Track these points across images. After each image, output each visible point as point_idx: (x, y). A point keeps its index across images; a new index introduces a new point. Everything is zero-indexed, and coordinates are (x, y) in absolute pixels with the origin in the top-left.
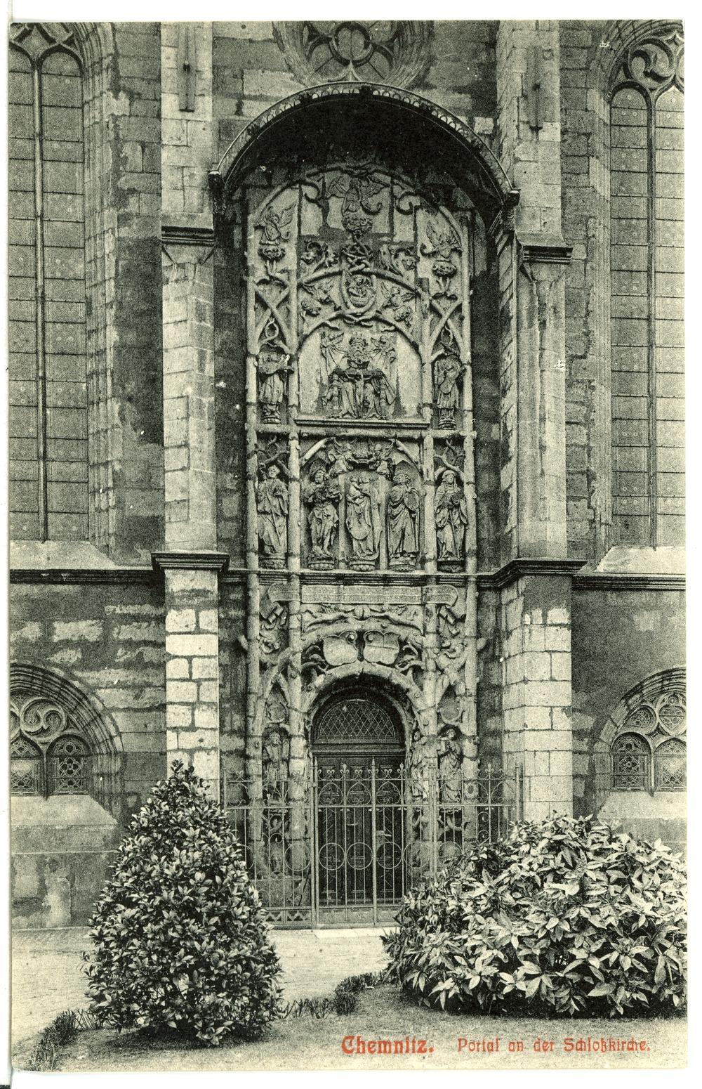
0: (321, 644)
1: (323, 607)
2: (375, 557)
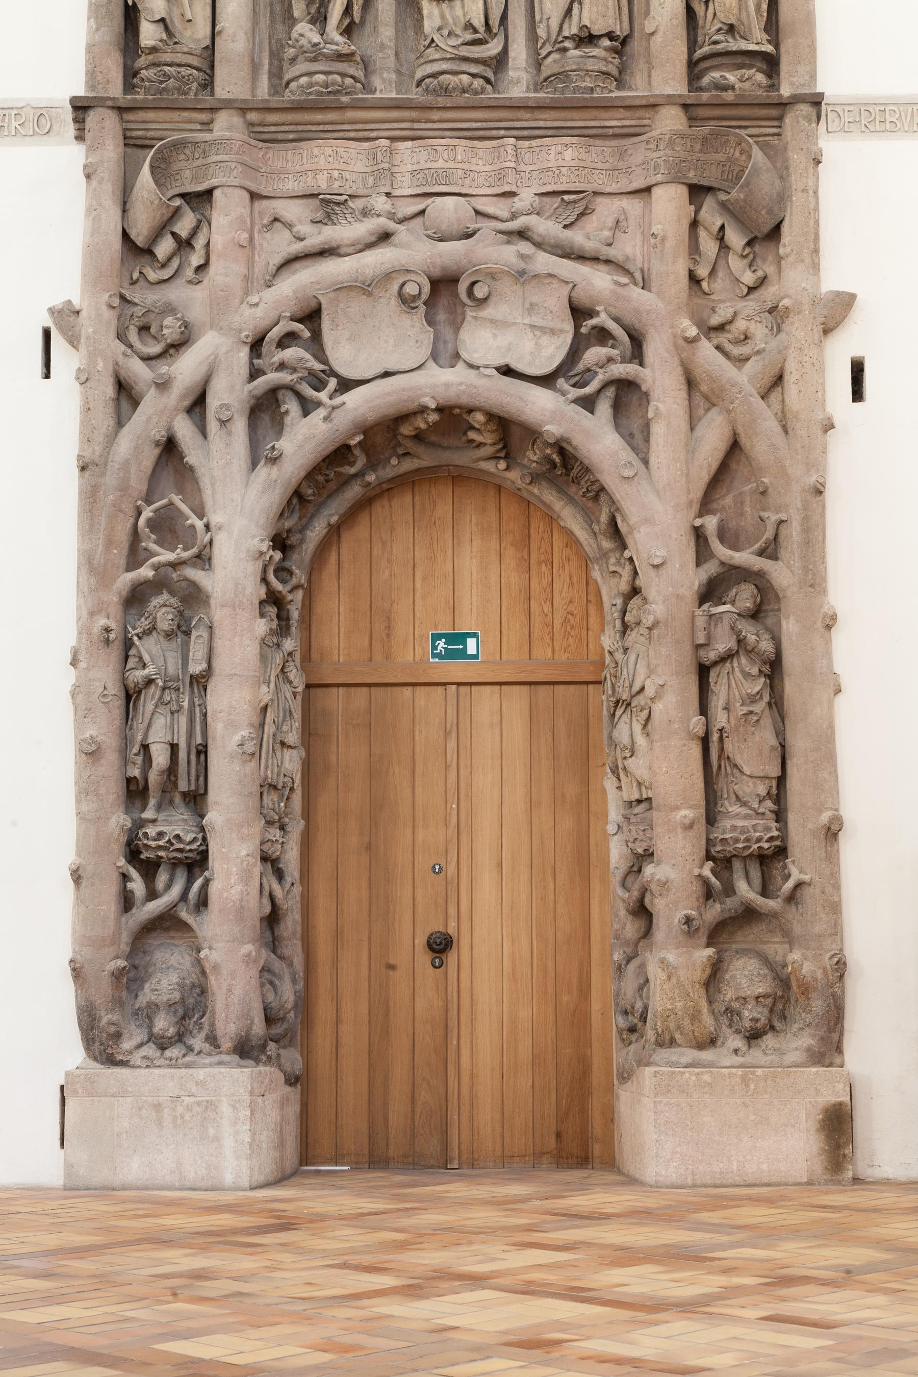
0: (312, 316)
1: (330, 206)
2: (493, 48)
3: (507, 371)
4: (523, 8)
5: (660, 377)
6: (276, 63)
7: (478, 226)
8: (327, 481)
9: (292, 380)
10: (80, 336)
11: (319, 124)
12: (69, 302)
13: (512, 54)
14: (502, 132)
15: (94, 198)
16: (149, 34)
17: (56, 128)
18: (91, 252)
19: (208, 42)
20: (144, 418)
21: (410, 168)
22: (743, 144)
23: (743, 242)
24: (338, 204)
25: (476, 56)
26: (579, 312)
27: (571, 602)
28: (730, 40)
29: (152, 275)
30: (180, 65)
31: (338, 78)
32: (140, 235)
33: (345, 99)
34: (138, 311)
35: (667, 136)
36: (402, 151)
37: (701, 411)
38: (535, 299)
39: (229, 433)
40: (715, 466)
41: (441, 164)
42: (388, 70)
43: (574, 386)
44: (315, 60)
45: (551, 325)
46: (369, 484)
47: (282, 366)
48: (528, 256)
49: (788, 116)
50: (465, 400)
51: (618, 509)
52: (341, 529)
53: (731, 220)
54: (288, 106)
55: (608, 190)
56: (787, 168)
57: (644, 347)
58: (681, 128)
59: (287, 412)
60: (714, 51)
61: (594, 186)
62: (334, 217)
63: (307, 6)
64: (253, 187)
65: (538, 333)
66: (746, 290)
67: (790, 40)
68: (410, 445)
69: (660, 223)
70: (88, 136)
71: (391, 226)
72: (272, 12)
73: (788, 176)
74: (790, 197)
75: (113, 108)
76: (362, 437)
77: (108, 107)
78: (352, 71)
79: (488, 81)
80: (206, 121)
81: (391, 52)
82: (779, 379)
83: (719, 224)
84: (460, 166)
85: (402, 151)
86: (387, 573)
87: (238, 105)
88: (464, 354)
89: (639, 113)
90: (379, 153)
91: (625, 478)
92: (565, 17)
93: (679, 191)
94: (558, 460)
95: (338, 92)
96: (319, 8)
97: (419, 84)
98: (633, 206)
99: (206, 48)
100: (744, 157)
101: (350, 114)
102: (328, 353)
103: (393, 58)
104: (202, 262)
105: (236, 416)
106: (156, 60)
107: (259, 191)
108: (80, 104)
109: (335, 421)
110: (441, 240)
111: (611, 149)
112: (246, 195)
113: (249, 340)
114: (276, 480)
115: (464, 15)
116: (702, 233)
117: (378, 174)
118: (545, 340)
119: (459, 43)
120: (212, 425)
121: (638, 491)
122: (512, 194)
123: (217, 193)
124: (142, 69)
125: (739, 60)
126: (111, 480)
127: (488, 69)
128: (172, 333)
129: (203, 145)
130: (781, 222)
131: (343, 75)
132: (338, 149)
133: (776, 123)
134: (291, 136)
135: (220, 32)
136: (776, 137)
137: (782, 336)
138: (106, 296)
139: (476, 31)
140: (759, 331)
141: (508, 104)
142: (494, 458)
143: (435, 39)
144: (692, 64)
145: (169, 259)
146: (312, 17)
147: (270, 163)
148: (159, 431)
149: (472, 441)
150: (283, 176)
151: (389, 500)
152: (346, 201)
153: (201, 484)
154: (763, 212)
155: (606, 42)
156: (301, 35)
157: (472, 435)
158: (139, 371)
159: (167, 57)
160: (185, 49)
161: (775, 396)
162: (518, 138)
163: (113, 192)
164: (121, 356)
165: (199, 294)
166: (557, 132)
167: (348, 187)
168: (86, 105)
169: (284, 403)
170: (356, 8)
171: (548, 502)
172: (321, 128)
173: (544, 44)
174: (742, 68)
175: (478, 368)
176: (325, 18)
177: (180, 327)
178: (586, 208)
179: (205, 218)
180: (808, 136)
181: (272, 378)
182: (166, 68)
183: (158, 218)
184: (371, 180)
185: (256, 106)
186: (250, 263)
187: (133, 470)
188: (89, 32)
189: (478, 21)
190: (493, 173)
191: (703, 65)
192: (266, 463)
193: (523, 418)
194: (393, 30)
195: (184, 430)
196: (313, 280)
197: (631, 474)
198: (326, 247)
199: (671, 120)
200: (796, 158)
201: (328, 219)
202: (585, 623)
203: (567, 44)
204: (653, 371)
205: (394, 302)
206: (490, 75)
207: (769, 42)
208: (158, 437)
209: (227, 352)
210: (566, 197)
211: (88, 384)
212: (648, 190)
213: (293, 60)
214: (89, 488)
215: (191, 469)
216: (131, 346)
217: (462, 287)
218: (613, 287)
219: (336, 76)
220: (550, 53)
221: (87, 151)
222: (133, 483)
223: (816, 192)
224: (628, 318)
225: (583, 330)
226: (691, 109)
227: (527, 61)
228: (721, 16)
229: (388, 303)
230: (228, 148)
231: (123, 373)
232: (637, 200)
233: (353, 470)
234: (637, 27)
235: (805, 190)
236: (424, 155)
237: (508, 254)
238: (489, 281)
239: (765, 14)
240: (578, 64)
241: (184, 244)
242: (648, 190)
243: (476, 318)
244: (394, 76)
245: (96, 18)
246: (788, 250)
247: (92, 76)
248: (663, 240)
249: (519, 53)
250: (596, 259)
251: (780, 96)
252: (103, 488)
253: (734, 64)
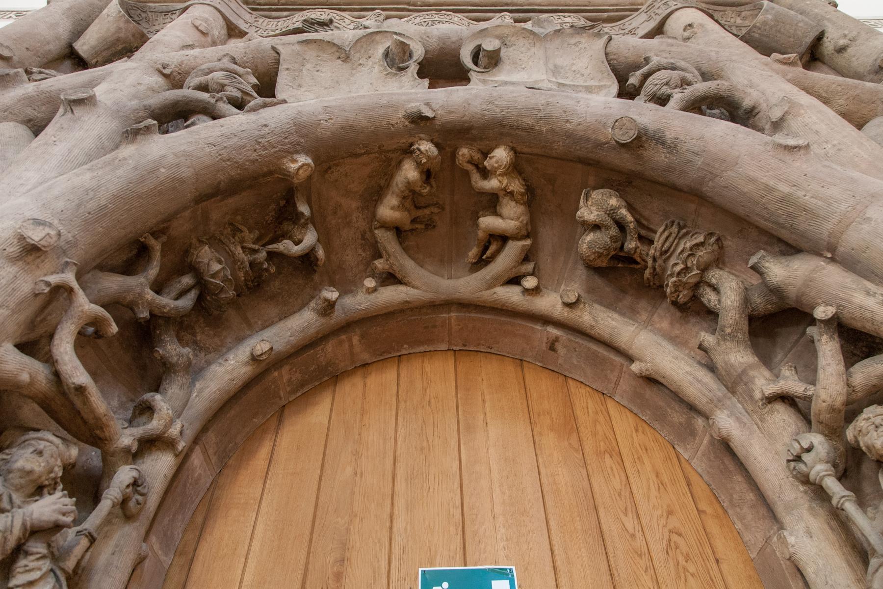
27: (670, 513)
38: (560, 61)
52: (286, 412)
86: (349, 471)
151: (365, 377)
202: (708, 550)
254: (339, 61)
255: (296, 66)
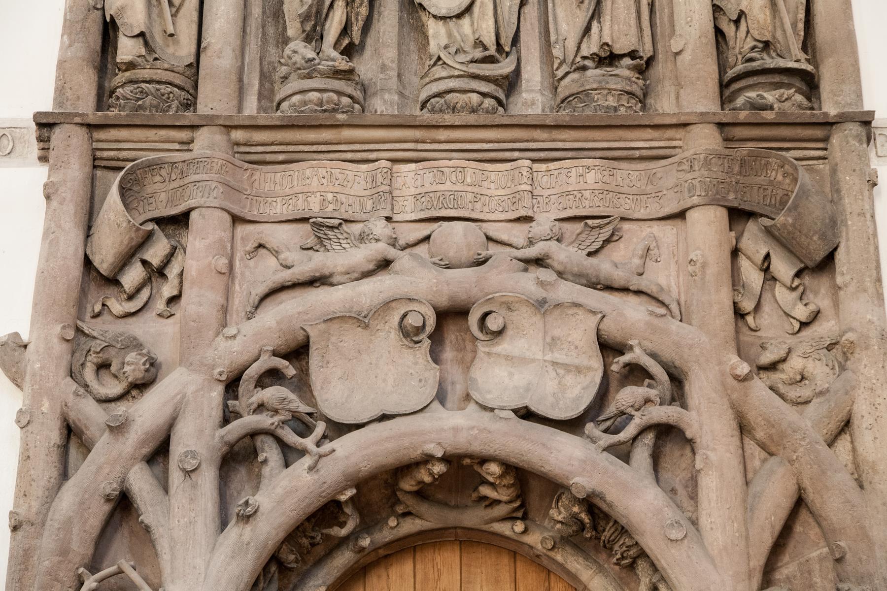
0: (298, 352)
1: (322, 229)
2: (505, 67)
3: (526, 414)
4: (537, 30)
5: (706, 419)
6: (267, 85)
7: (490, 252)
8: (313, 545)
9: (273, 424)
10: (25, 372)
11: (313, 144)
12: (16, 335)
13: (525, 75)
14: (516, 154)
15: (52, 217)
16: (127, 49)
17: (18, 148)
18: (44, 279)
19: (192, 59)
20: (93, 468)
21: (413, 191)
22: (787, 167)
23: (793, 272)
24: (332, 228)
25: (487, 73)
26: (609, 348)
28: (765, 56)
29: (117, 306)
30: (159, 82)
31: (334, 97)
32: (104, 261)
33: (341, 117)
34: (97, 345)
35: (702, 156)
36: (405, 174)
37: (757, 463)
38: (557, 332)
39: (194, 486)
40: (778, 528)
41: (448, 186)
42: (389, 91)
43: (606, 431)
44: (309, 76)
45: (577, 362)
46: (363, 549)
47: (261, 407)
48: (549, 284)
49: (835, 136)
50: (477, 447)
51: (663, 579)
53: (777, 248)
54: (278, 123)
55: (636, 216)
56: (838, 191)
57: (687, 387)
58: (717, 148)
59: (265, 461)
60: (750, 69)
61: (622, 212)
62: (326, 242)
63: (302, 23)
64: (236, 210)
65: (561, 372)
66: (797, 326)
67: (831, 60)
68: (411, 503)
69: (698, 248)
70: (52, 154)
71: (392, 253)
72: (264, 34)
73: (840, 199)
74: (844, 222)
75: (82, 125)
76: (354, 491)
77: (76, 124)
78: (349, 90)
79: (500, 103)
80: (185, 140)
81: (393, 74)
82: (846, 425)
83: (763, 252)
84: (469, 189)
85: (405, 174)
87: (221, 122)
88: (475, 395)
89: (670, 133)
90: (379, 176)
91: (672, 541)
92: (583, 36)
93: (718, 214)
94: (587, 520)
95: (334, 110)
96: (315, 26)
97: (423, 106)
98: (667, 232)
99: (190, 65)
100: (788, 181)
101: (347, 133)
102: (316, 393)
103: (395, 79)
104: (175, 293)
105: (204, 466)
106: (133, 77)
107: (242, 215)
108: (44, 121)
109: (322, 472)
110: (448, 268)
111: (637, 173)
112: (227, 218)
113: (224, 377)
114: (248, 543)
115: (474, 32)
116: (744, 262)
117: (376, 197)
118: (570, 379)
119: (468, 59)
120: (176, 477)
121: (689, 557)
122: (528, 219)
123: (194, 215)
124: (119, 87)
125: (777, 78)
126: (48, 542)
127: (500, 90)
128: (134, 370)
129: (181, 164)
130: (836, 249)
131: (340, 93)
132: (333, 171)
133: (821, 145)
134: (281, 157)
135: (205, 48)
136: (821, 161)
137: (848, 374)
138: (58, 328)
139: (486, 48)
140: (820, 371)
141: (523, 122)
142: (510, 518)
143: (442, 56)
144: (723, 86)
145: (138, 290)
146: (308, 35)
147: (256, 185)
148: (111, 483)
149: (485, 498)
150: (270, 200)
151: (387, 569)
152: (340, 224)
153: (159, 548)
154: (815, 238)
155: (627, 61)
156: (295, 52)
157: (485, 491)
158: (91, 414)
159: (146, 74)
160: (166, 66)
161: (843, 444)
162: (534, 161)
163: (75, 213)
164: (71, 396)
165: (170, 327)
166: (579, 152)
167: (343, 210)
168: (52, 121)
169: (263, 451)
170: (355, 28)
171: (573, 571)
172: (314, 148)
173: (561, 64)
174: (780, 88)
175: (492, 410)
176: (322, 37)
177: (144, 364)
178: (612, 235)
179: (182, 245)
180: (860, 157)
181: (250, 421)
182: (143, 85)
183: (125, 242)
184: (369, 205)
185: (241, 123)
186: (228, 294)
187: (75, 530)
188: (61, 49)
189: (489, 39)
190: (506, 198)
191: (736, 86)
192: (237, 522)
193: (546, 469)
194: (396, 52)
195: (141, 482)
196: (300, 309)
197: (680, 536)
198: (317, 274)
199: (704, 139)
200: (849, 181)
201: (321, 243)
203: (588, 63)
204: (699, 414)
205: (394, 336)
206: (501, 95)
207: (808, 61)
208: (108, 491)
209: (197, 391)
210: (590, 222)
211: (29, 428)
212: (681, 215)
213: (285, 78)
214: (21, 553)
215: (147, 529)
216: (86, 386)
217: (473, 319)
218: (648, 318)
219: (331, 94)
220: (567, 73)
221: (50, 171)
222: (75, 546)
223: (873, 216)
224: (668, 354)
225: (615, 368)
226: (727, 129)
227: (542, 83)
228: (755, 34)
229: (387, 336)
230: (209, 166)
231: (72, 416)
232: (670, 227)
233: (344, 532)
234: (660, 49)
235: (862, 214)
236: (429, 177)
237: (528, 283)
238: (503, 312)
239: (802, 33)
240: (600, 82)
241: (158, 273)
242: (681, 215)
243: (489, 354)
244: (396, 97)
245: (70, 35)
246: (847, 278)
247: (60, 91)
248: (704, 266)
249: (533, 74)
250: (625, 290)
251: (826, 114)
252: (38, 552)
253: (771, 83)
254: (359, 329)
255: (323, 343)
